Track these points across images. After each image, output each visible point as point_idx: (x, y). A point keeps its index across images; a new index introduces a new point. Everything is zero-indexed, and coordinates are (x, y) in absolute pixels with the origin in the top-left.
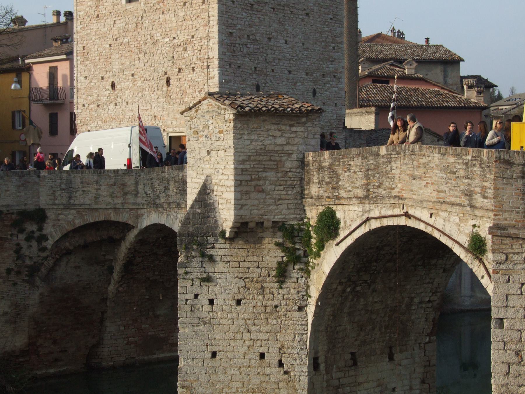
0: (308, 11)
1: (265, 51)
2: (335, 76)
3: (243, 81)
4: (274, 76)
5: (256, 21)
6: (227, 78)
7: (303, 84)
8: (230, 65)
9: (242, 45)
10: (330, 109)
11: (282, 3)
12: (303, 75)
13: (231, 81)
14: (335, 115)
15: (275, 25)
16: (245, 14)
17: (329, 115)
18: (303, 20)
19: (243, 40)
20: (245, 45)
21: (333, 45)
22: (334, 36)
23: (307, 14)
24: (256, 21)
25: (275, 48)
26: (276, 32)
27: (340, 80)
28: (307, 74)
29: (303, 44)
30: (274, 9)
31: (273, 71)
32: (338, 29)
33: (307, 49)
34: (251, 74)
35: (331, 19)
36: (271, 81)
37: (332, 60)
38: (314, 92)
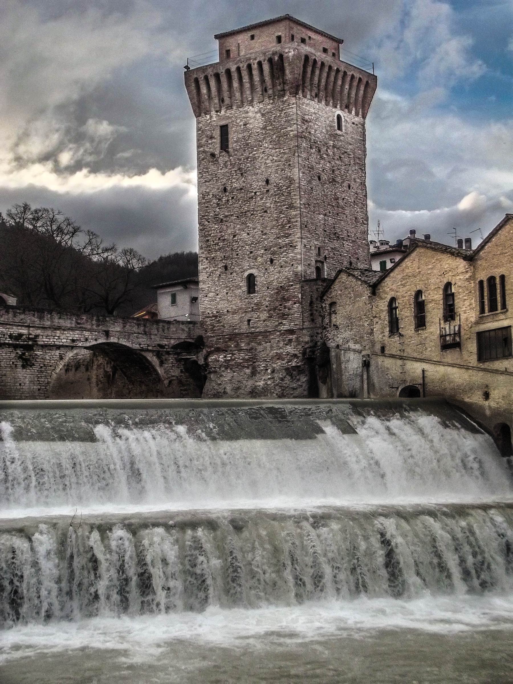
0: (265, 209)
1: (231, 244)
2: (291, 246)
3: (216, 266)
4: (238, 258)
5: (225, 228)
6: (205, 266)
7: (262, 257)
8: (207, 259)
9: (215, 245)
10: (287, 269)
11: (244, 211)
12: (262, 251)
13: (207, 268)
14: (291, 273)
15: (238, 226)
16: (216, 226)
17: (286, 273)
18: (261, 216)
19: (215, 242)
20: (217, 244)
21: (289, 225)
22: (290, 218)
23: (266, 212)
24: (225, 228)
25: (239, 240)
26: (239, 230)
27: (297, 247)
28: (266, 250)
29: (262, 232)
30: (238, 217)
31: (237, 255)
32: (293, 213)
33: (265, 234)
34: (221, 260)
35: (287, 208)
36: (236, 261)
37: (287, 236)
38: (272, 261)
